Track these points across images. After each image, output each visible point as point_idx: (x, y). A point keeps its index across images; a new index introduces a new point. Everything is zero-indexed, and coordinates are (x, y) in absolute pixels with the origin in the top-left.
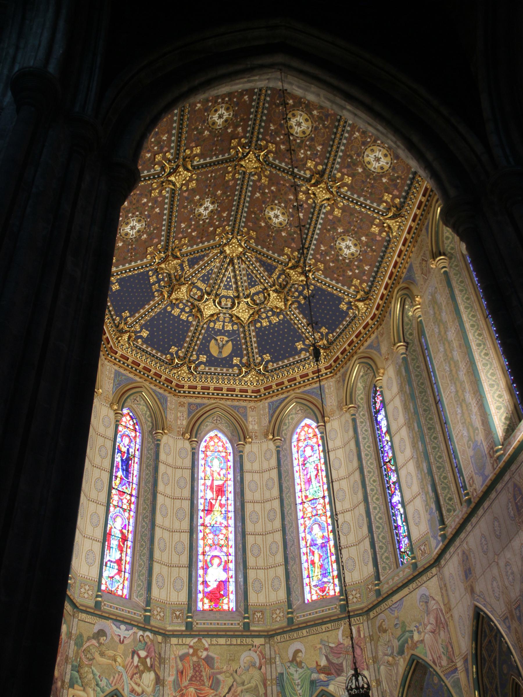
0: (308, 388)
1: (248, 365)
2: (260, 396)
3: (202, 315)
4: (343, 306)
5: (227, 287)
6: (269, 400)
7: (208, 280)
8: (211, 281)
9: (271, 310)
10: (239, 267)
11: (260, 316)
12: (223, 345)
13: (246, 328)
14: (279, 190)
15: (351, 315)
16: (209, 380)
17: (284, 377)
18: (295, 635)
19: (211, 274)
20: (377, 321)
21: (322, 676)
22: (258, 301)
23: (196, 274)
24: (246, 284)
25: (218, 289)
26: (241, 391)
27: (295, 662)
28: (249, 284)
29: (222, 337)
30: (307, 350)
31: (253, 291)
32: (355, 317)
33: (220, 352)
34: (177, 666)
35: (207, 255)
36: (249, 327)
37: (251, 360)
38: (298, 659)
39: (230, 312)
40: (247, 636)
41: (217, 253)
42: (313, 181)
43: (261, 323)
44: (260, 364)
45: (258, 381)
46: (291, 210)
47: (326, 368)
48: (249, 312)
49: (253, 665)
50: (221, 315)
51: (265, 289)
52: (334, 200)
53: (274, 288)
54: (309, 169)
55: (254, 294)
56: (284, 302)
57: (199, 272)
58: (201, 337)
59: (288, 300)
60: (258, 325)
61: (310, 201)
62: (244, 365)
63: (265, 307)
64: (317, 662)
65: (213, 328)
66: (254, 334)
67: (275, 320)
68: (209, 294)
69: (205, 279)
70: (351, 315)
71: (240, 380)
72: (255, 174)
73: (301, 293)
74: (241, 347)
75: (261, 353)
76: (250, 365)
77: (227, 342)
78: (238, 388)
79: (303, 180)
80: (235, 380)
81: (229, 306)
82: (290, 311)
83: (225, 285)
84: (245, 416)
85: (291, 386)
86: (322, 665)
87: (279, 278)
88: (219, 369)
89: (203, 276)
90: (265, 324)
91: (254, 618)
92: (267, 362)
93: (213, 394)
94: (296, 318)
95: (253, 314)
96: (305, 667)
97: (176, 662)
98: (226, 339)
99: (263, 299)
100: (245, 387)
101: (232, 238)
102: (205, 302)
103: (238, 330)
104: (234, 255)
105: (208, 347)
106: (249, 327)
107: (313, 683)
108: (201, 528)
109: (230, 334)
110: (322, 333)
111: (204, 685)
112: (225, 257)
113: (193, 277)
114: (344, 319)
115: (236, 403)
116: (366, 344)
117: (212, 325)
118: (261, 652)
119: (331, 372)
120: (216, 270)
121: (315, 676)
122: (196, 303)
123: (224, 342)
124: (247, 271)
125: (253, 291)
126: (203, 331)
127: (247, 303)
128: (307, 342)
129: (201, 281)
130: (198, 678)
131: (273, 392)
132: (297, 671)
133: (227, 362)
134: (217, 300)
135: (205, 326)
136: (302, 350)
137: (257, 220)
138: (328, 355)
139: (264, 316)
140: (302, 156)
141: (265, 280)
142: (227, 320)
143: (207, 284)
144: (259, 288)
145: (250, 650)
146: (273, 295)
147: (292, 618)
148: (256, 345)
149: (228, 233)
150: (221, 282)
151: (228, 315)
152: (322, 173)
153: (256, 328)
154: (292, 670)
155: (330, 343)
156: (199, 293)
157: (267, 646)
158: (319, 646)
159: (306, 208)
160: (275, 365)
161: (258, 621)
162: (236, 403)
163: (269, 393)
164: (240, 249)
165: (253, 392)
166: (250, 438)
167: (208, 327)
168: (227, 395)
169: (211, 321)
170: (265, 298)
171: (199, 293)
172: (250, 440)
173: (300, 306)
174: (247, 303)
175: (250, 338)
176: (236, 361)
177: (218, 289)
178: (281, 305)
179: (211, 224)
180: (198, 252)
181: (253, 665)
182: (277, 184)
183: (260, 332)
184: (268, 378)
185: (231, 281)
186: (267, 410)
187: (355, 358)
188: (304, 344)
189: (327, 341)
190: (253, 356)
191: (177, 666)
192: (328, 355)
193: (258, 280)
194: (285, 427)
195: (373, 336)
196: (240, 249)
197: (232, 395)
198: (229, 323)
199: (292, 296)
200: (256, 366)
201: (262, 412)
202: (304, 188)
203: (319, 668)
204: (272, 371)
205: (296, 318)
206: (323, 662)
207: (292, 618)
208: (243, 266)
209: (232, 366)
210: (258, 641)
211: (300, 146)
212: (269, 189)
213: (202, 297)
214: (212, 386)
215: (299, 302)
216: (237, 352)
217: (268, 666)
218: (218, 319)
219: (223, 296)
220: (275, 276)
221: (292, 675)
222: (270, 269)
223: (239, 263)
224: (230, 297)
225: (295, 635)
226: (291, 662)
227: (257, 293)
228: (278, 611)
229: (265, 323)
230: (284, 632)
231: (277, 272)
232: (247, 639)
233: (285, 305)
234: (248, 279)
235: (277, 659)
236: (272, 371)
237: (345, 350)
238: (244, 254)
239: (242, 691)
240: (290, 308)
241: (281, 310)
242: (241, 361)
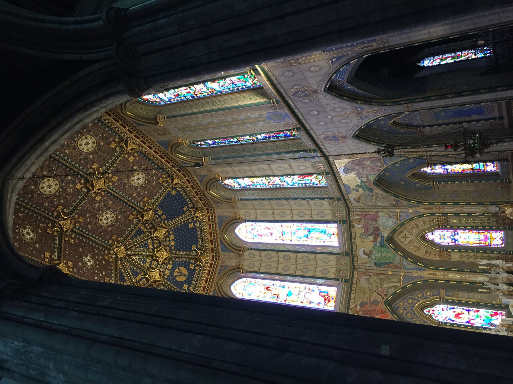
0: (217, 226)
1: (196, 260)
2: (216, 256)
3: (158, 281)
4: (174, 193)
5: (145, 262)
6: (220, 251)
7: (136, 272)
8: (138, 271)
9: (166, 237)
10: (134, 251)
11: (168, 246)
12: (180, 272)
13: (173, 255)
14: (90, 212)
15: (180, 189)
16: (199, 285)
17: (208, 239)
18: (355, 252)
19: (133, 270)
20: (187, 174)
21: (379, 239)
22: (158, 245)
23: (131, 279)
24: (145, 250)
25: (144, 268)
26: (211, 267)
27: (370, 255)
28: (146, 248)
29: (175, 272)
30: (195, 222)
31: (151, 246)
32: (182, 187)
33: (184, 275)
35: (120, 269)
36: (173, 254)
37: (193, 257)
38: (368, 253)
39: (161, 263)
40: (352, 281)
41: (121, 263)
42: (91, 188)
43: (172, 246)
44: (197, 252)
45: (207, 256)
46: (105, 208)
47: (208, 213)
48: (163, 251)
49: (368, 280)
50: (161, 269)
51: (151, 238)
52: (106, 178)
53: (153, 233)
54: (82, 188)
55: (153, 246)
56: (162, 228)
57: (130, 277)
58: (172, 285)
59: (162, 226)
60: (173, 248)
61: (103, 194)
62: (196, 262)
63: (163, 241)
65: (168, 276)
66: (178, 252)
67: (172, 237)
68: (146, 274)
69: (136, 274)
70: (180, 189)
71: (204, 266)
72: (75, 225)
73: (160, 217)
74: (184, 261)
75: (190, 250)
76: (196, 259)
77: (179, 269)
78: (208, 268)
79: (88, 194)
80: (203, 270)
81: (157, 263)
82: (169, 226)
83: (143, 263)
84: (227, 266)
85: (214, 236)
87: (146, 228)
88: (194, 278)
89: (133, 275)
90: (173, 244)
91: (342, 276)
92: (197, 248)
93: (209, 284)
94: (174, 223)
95: (165, 250)
98: (177, 270)
99: (157, 242)
100: (209, 264)
101: (113, 251)
102: (150, 277)
103: (173, 261)
104: (125, 252)
105: (179, 282)
106: (173, 254)
107: (381, 246)
108: (287, 303)
109: (174, 266)
110: (187, 211)
112: (125, 258)
113: (132, 281)
114: (181, 195)
115: (217, 271)
116: (199, 184)
117: (166, 277)
118: (362, 274)
119: (211, 210)
120: (132, 267)
121: (378, 244)
122: (150, 283)
123: (179, 272)
124: (137, 247)
125: (151, 246)
126: (169, 283)
127: (158, 251)
128: (190, 221)
129: (136, 277)
131: (215, 247)
132: (374, 254)
133: (191, 273)
134: (151, 270)
135: (166, 281)
136: (194, 225)
137: (105, 231)
138: (201, 210)
139: (168, 243)
140: (71, 190)
141: (146, 237)
142: (165, 266)
143: (139, 274)
144: (150, 242)
145: (360, 280)
146: (156, 234)
147: (346, 253)
148: (185, 252)
149: (110, 253)
150: (140, 265)
151: (162, 266)
152: (87, 181)
153: (174, 250)
154: (373, 257)
155: (194, 206)
156: (144, 280)
157: (359, 270)
158: (363, 239)
159: (107, 198)
160: (199, 243)
161: (345, 273)
162: (217, 271)
163: (216, 250)
164: (122, 247)
165: (213, 260)
166: (240, 265)
167: (167, 279)
168: (211, 276)
169: (163, 277)
170: (157, 240)
171: (144, 280)
172: (241, 265)
173: (167, 219)
174: (158, 251)
175: (180, 254)
176: (192, 267)
177: (144, 268)
178: (164, 231)
179: (101, 261)
180: (117, 274)
181: (368, 280)
182: (86, 212)
183: (177, 248)
184: (206, 249)
185: (141, 259)
186: (226, 253)
187: (205, 192)
188: (191, 223)
189: (192, 208)
190: (191, 255)
192: (201, 210)
193: (145, 242)
194: (238, 243)
195: (196, 178)
196: (122, 247)
197: (212, 273)
198: (167, 266)
199: (160, 223)
200: (197, 255)
201: (226, 256)
202: (93, 195)
203: (374, 241)
204: (203, 246)
205: (174, 223)
206: (372, 238)
207: (346, 253)
208: (134, 248)
209: (194, 270)
210: (356, 275)
211: (64, 190)
212: (87, 218)
213: (146, 279)
214: (203, 284)
215: (165, 219)
216: (186, 265)
217: (370, 271)
218: (163, 272)
219: (150, 265)
220: (145, 230)
221: (376, 257)
222: (140, 232)
223: (131, 251)
224: (151, 261)
225: (355, 252)
226: (369, 257)
227: (153, 244)
228: (341, 261)
229: (173, 243)
230: (353, 259)
231: (143, 228)
232: (354, 281)
233: (164, 228)
234: (142, 248)
235: (366, 265)
236: (203, 246)
237: (200, 198)
238: (126, 246)
239: (381, 288)
240: (167, 226)
241: (167, 231)
242: (193, 264)
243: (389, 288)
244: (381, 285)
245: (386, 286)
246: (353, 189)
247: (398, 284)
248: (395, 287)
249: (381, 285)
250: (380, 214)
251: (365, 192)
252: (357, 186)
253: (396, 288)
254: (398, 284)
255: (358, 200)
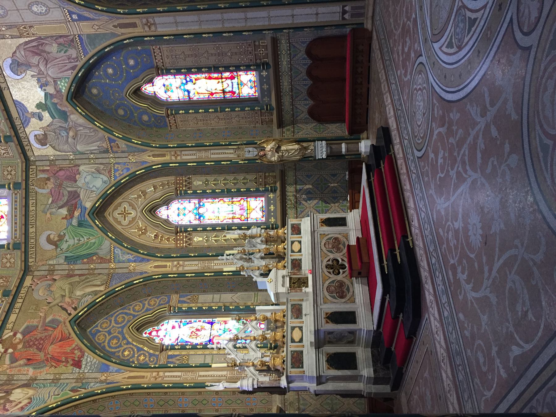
34: (20, 366)
64: (63, 218)
86: (66, 213)
96: (65, 232)
97: (15, 367)
107: (80, 225)
111: (50, 336)
121: (75, 222)
130: (42, 342)
191: (20, 366)
203: (68, 217)
206: (64, 211)
221: (69, 246)
239: (70, 297)
243: (85, 295)
244: (71, 292)
245: (78, 293)
246: (33, 114)
247: (102, 288)
248: (95, 293)
249: (71, 292)
250: (81, 168)
251: (55, 120)
252: (39, 106)
253: (96, 295)
254: (102, 288)
255: (43, 140)
